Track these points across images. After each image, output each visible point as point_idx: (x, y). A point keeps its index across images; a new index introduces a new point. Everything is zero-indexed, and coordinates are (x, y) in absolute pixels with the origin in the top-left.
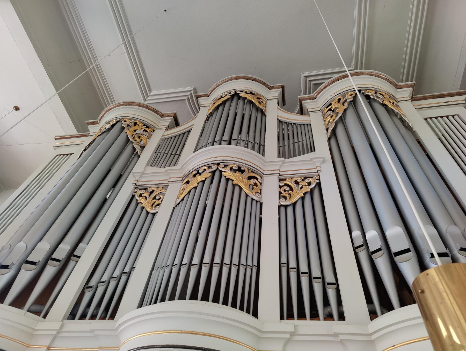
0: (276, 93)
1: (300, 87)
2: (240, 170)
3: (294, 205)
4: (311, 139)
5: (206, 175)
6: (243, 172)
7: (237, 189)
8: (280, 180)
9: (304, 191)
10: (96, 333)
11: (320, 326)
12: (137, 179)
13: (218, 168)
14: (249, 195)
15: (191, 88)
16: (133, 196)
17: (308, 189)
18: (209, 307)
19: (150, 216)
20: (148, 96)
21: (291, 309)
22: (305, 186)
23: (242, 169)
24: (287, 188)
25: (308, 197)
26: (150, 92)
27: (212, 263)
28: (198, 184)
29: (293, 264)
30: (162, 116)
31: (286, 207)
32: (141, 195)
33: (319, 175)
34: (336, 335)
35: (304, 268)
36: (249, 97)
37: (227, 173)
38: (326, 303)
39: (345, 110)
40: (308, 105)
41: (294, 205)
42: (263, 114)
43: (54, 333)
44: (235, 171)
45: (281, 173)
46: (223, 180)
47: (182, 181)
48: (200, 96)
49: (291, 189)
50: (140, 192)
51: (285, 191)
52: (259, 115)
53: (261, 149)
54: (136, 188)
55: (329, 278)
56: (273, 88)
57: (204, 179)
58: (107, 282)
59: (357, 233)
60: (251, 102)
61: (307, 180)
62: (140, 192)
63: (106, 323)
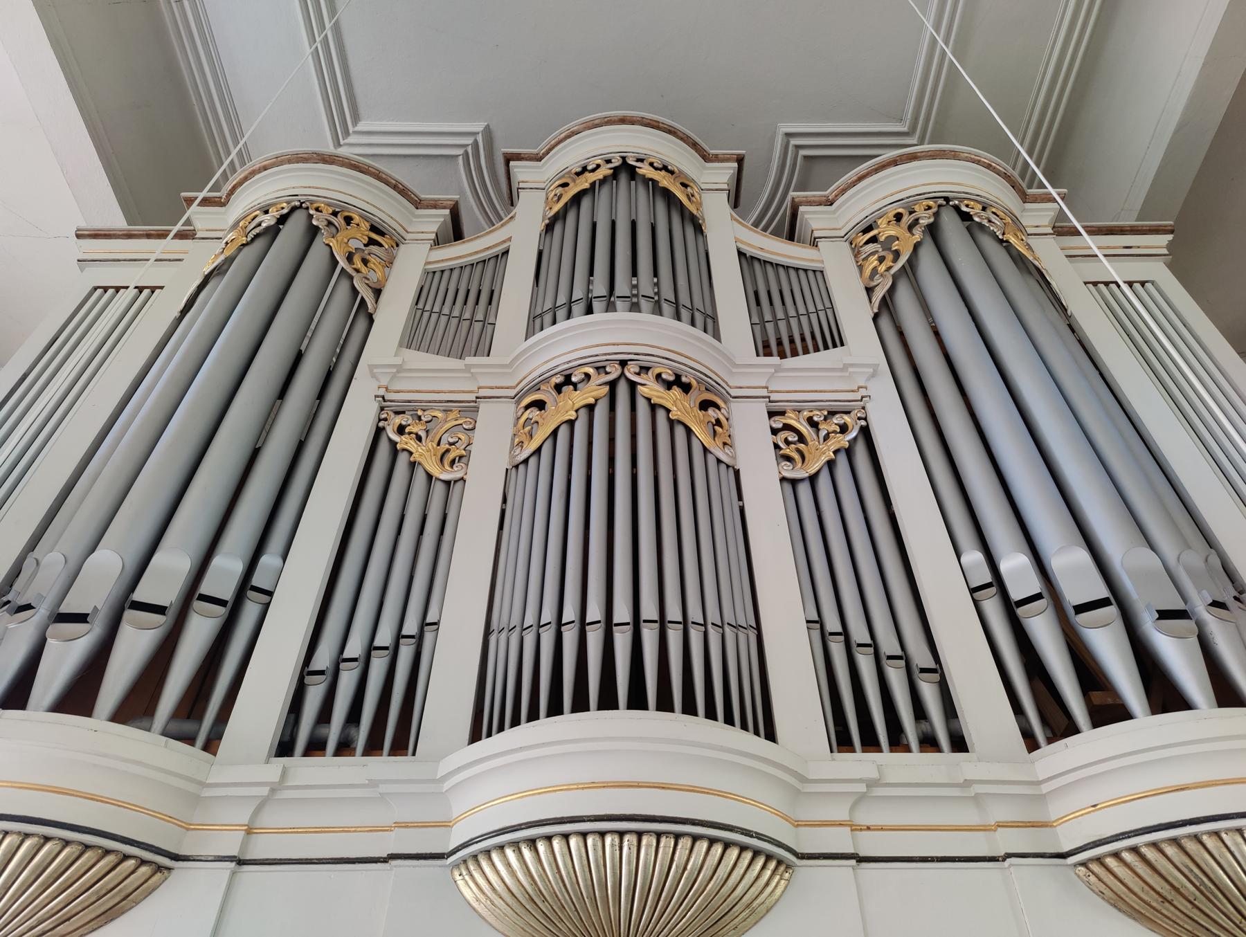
0: (723, 174)
1: (770, 161)
2: (678, 383)
3: (813, 479)
4: (829, 312)
5: (594, 390)
6: (686, 388)
8: (771, 414)
9: (834, 444)
10: (383, 788)
11: (912, 766)
12: (384, 382)
13: (623, 374)
14: (712, 450)
15: (478, 127)
16: (379, 431)
17: (844, 441)
18: (676, 723)
19: (438, 489)
20: (347, 133)
21: (852, 728)
22: (834, 432)
23: (684, 379)
24: (792, 437)
25: (842, 462)
26: (355, 123)
27: (662, 622)
28: (576, 411)
29: (833, 624)
30: (418, 204)
31: (794, 482)
32: (401, 430)
33: (863, 408)
34: (967, 783)
35: (859, 633)
36: (664, 180)
37: (650, 389)
38: (920, 712)
39: (917, 247)
40: (813, 219)
41: (813, 479)
42: (699, 229)
43: (264, 791)
44: (669, 385)
45: (774, 397)
46: (642, 407)
47: (517, 398)
48: (518, 157)
49: (802, 439)
50: (398, 420)
51: (787, 442)
52: (690, 231)
53: (710, 323)
54: (382, 409)
55: (921, 658)
56: (716, 159)
57: (592, 401)
58: (362, 660)
59: (973, 557)
60: (667, 195)
61: (837, 419)
62: (398, 420)
63: (384, 766)
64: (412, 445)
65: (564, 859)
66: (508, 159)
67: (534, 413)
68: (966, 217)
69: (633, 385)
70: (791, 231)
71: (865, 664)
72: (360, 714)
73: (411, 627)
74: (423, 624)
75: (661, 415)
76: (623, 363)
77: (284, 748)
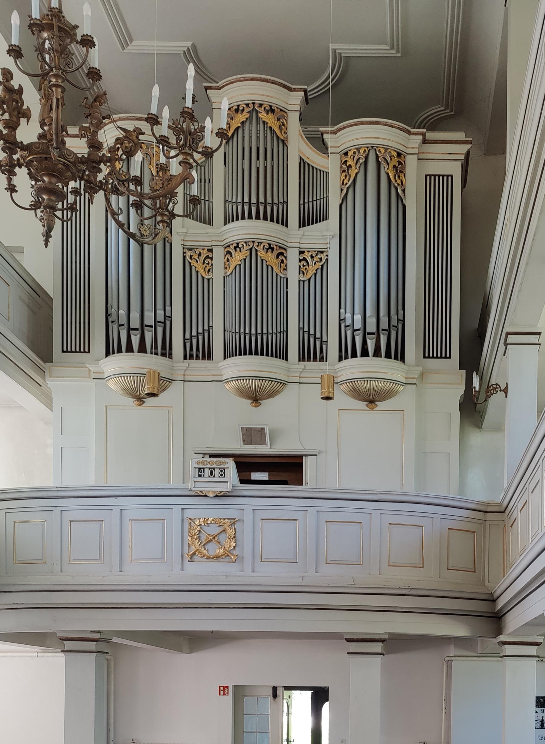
3: (309, 280)
7: (270, 268)
8: (301, 253)
9: (316, 267)
15: (189, 44)
16: (184, 257)
17: (319, 265)
24: (305, 264)
35: (312, 332)
38: (321, 351)
39: (357, 174)
41: (309, 280)
48: (210, 88)
51: (304, 266)
56: (295, 90)
64: (195, 264)
65: (244, 383)
66: (207, 88)
67: (228, 256)
68: (377, 157)
69: (256, 251)
70: (321, 146)
71: (312, 340)
72: (199, 350)
73: (206, 328)
74: (209, 327)
75: (264, 262)
76: (253, 242)
77: (185, 358)
